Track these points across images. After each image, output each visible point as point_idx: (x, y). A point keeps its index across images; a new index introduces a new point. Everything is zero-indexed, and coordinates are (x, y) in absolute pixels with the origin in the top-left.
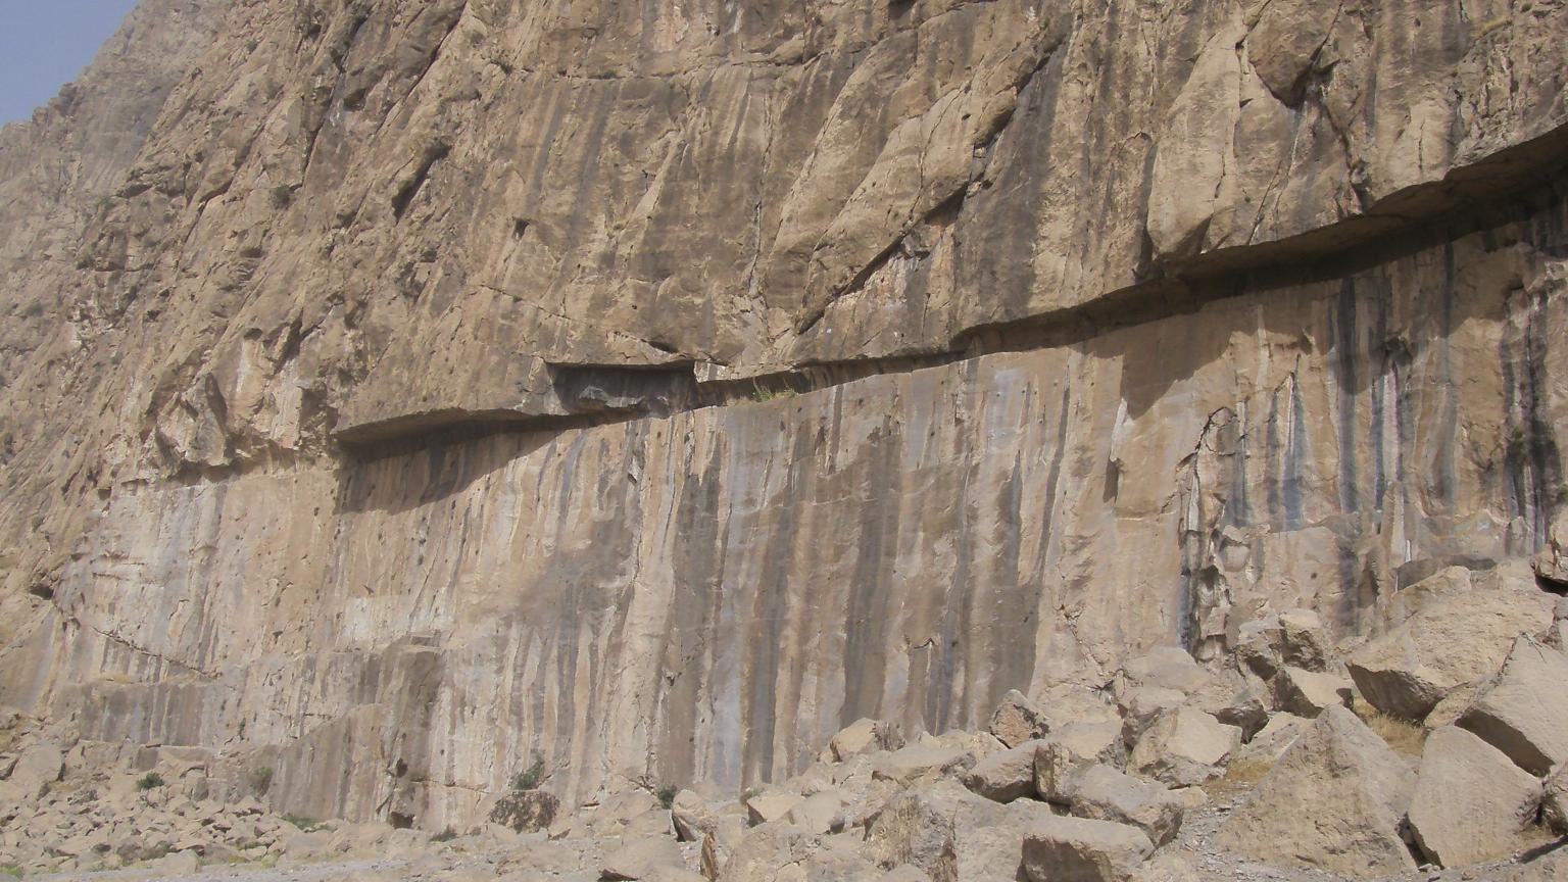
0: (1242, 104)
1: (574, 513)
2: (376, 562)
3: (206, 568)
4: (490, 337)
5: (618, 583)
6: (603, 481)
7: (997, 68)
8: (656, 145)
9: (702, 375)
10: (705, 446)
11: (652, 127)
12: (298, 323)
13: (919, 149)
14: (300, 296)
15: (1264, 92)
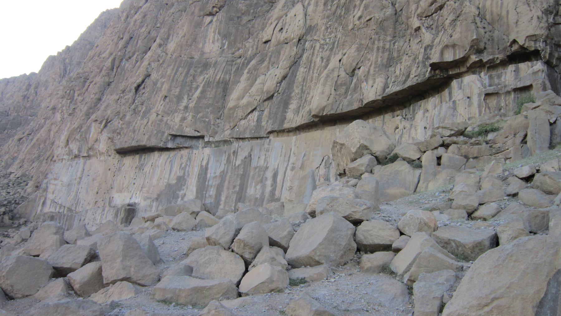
0: (338, 76)
1: (173, 173)
2: (123, 184)
3: (79, 183)
4: (155, 126)
5: (182, 192)
6: (181, 165)
7: (285, 62)
8: (202, 78)
9: (206, 139)
10: (206, 158)
11: (201, 72)
12: (107, 119)
13: (263, 83)
14: (109, 112)
15: (344, 73)
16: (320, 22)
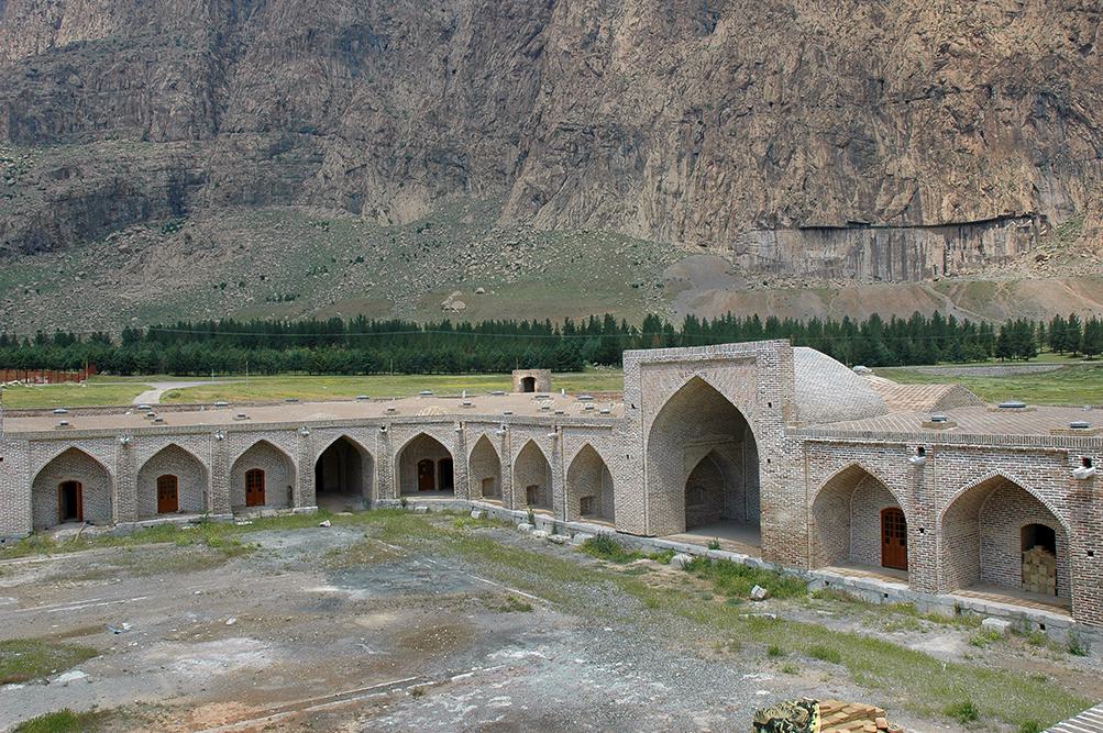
16: (924, 173)
